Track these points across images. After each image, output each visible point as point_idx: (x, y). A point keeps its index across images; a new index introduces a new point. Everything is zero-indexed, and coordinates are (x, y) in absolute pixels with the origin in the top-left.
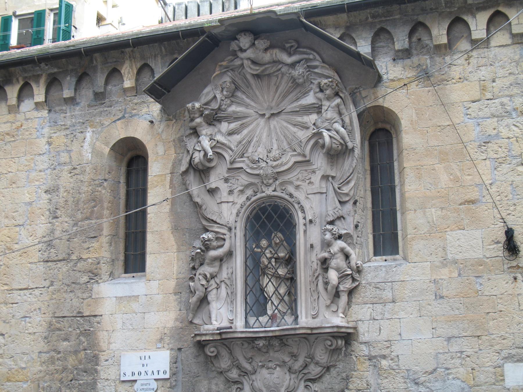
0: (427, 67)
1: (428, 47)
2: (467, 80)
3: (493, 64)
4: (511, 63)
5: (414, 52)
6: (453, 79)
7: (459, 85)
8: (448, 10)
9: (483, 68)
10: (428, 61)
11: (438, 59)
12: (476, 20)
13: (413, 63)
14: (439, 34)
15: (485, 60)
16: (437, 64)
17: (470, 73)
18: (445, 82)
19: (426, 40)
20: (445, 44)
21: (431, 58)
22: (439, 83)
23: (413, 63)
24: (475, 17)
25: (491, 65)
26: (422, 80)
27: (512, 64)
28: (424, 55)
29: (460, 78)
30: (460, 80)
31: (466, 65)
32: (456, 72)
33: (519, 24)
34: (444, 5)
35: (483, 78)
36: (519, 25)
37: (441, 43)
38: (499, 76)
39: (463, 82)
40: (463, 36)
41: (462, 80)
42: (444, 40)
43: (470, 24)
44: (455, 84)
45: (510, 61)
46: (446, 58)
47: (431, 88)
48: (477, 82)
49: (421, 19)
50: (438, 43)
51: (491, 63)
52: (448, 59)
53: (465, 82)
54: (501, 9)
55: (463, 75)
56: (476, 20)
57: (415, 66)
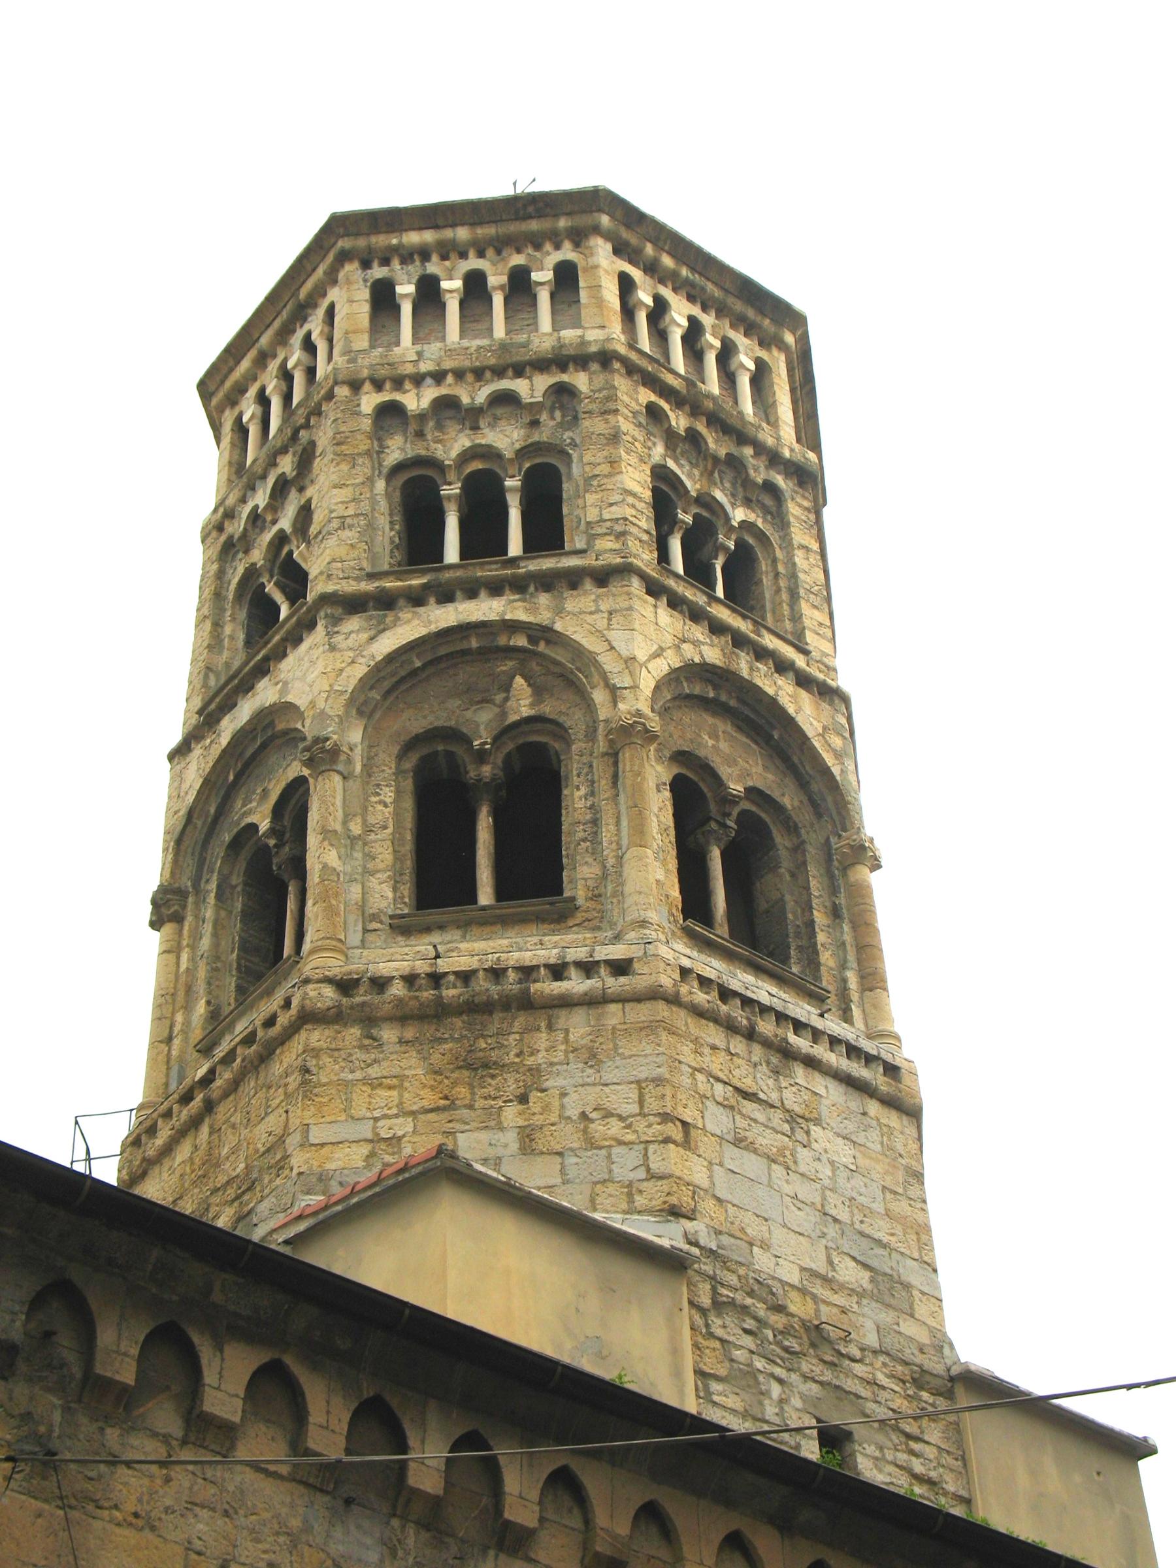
0: (50, 1431)
1: (65, 1370)
2: (153, 1528)
3: (231, 1511)
4: (277, 1534)
5: (22, 1367)
6: (116, 1507)
7: (127, 1536)
8: (154, 1290)
9: (204, 1514)
10: (57, 1417)
11: (86, 1426)
12: (223, 1360)
13: (11, 1399)
14: (120, 1350)
15: (212, 1490)
16: (81, 1436)
17: (167, 1510)
18: (90, 1507)
19: (66, 1347)
20: (125, 1388)
21: (66, 1409)
22: (73, 1502)
23: (11, 1399)
24: (222, 1351)
25: (226, 1514)
26: (28, 1469)
27: (282, 1539)
28: (49, 1390)
29: (136, 1515)
30: (134, 1521)
31: (159, 1481)
32: (129, 1487)
33: (327, 1428)
34: (150, 1267)
35: (198, 1544)
36: (325, 1432)
37: (117, 1377)
38: (243, 1560)
39: (142, 1529)
40: (168, 1388)
41: (140, 1523)
42: (127, 1375)
43: (204, 1361)
44: (118, 1525)
45: (276, 1527)
46: (109, 1431)
47: (46, 1507)
48: (179, 1550)
49: (77, 1274)
50: (109, 1374)
51: (227, 1507)
52: (112, 1435)
53: (147, 1533)
54: (288, 1360)
55: (148, 1508)
56: (223, 1360)
57: (16, 1412)
